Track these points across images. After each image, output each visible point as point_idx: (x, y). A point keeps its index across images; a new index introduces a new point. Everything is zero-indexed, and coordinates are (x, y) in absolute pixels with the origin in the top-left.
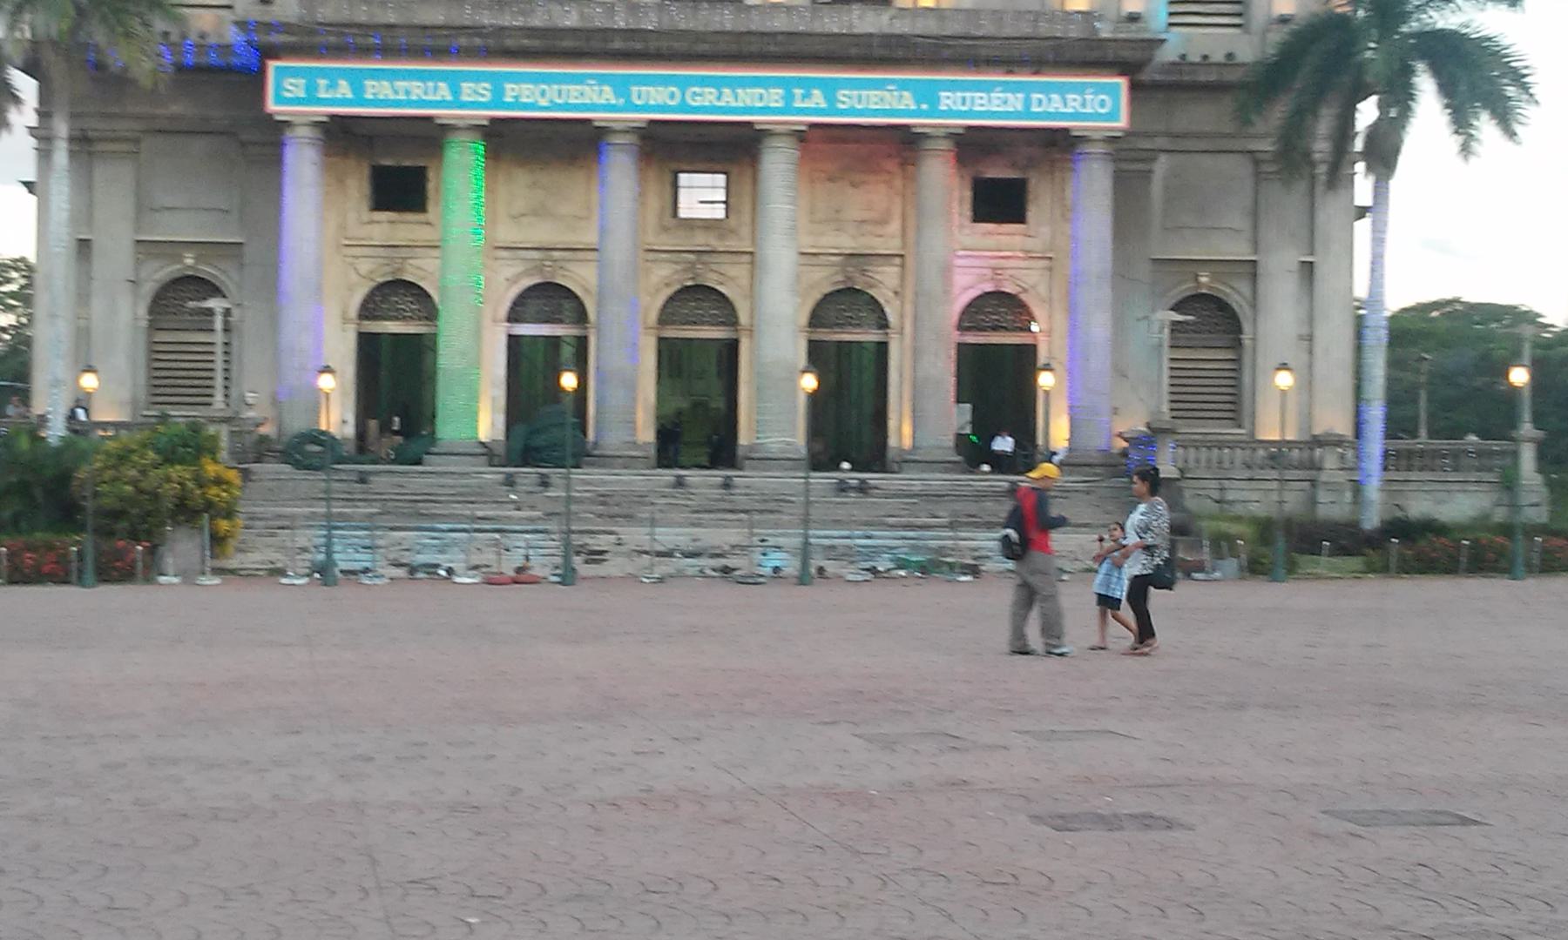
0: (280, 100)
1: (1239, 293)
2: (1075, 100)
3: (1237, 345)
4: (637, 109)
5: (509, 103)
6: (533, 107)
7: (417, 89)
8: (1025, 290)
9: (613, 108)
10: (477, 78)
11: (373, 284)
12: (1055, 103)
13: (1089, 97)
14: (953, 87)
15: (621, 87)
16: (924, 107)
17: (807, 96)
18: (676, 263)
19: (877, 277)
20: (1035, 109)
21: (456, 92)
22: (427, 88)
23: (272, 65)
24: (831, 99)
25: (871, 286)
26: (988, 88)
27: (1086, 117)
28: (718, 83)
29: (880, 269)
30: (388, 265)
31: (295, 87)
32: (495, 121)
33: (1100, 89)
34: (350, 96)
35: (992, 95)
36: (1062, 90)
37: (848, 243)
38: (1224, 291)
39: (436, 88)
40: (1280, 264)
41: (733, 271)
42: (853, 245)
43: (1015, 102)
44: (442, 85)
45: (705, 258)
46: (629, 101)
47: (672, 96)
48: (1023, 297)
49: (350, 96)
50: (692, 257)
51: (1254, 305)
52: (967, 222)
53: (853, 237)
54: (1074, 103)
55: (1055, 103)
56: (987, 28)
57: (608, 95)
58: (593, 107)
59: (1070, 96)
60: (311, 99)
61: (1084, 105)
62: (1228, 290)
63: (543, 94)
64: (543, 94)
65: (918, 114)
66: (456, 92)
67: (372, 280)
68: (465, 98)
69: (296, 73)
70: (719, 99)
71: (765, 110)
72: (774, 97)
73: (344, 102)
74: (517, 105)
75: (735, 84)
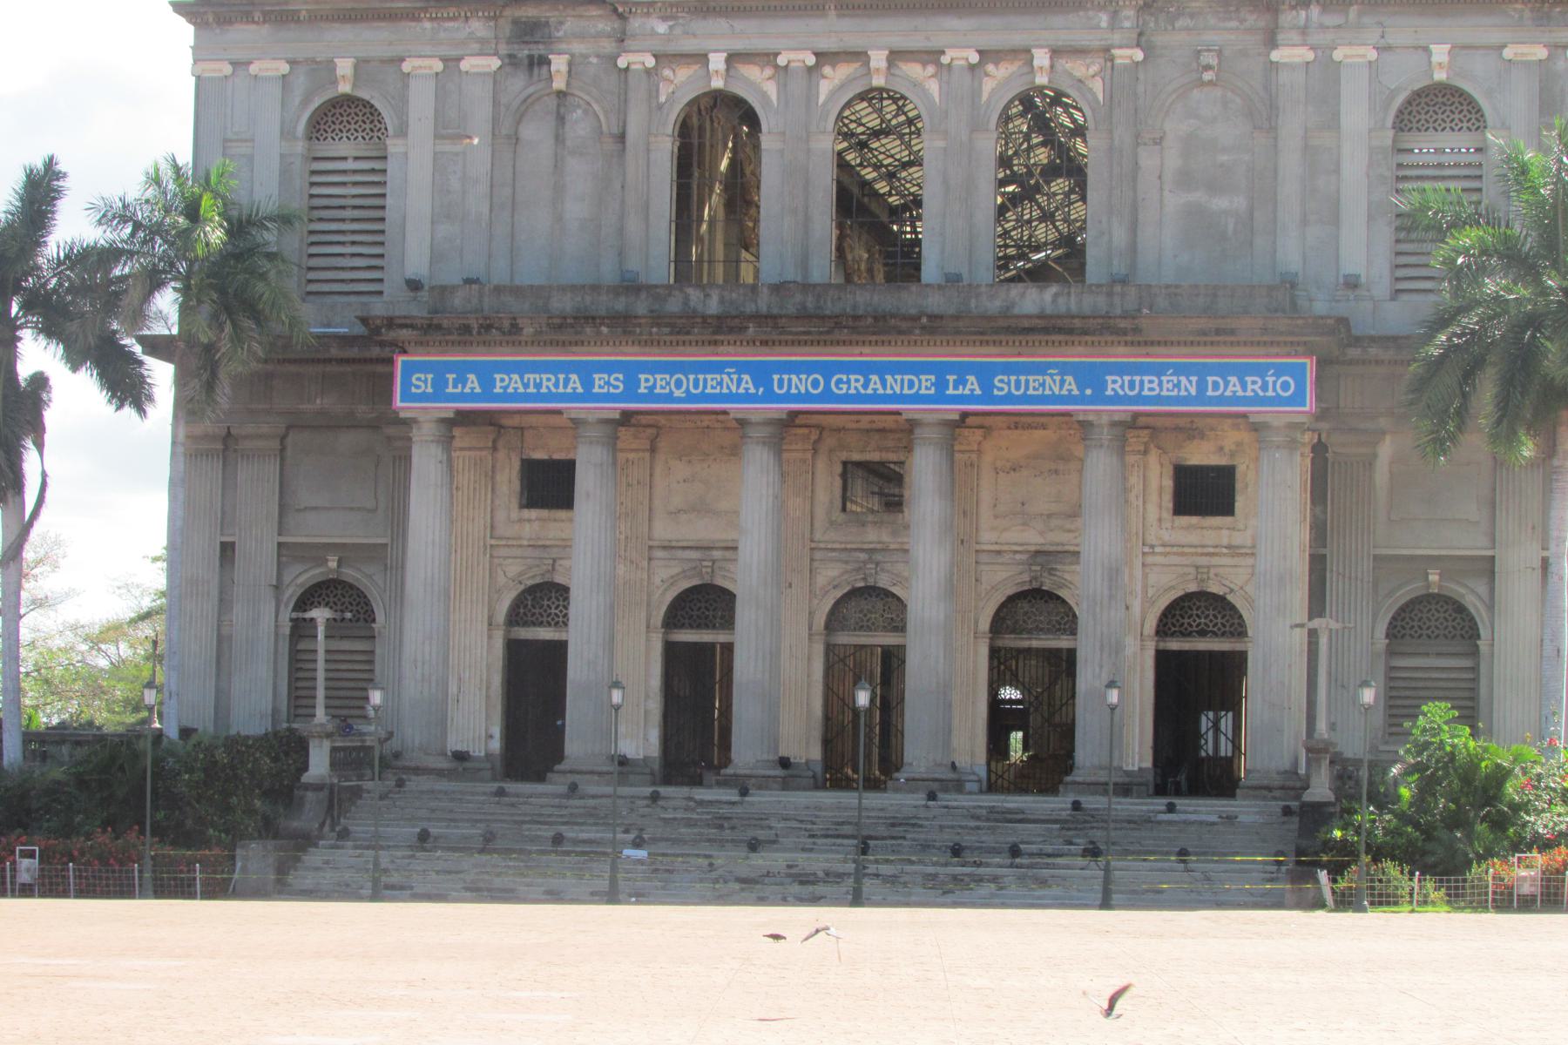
0: (407, 396)
1: (1473, 591)
2: (1254, 383)
3: (1474, 653)
5: (643, 394)
6: (669, 397)
7: (548, 382)
8: (1232, 590)
9: (748, 397)
10: (608, 368)
11: (522, 587)
13: (1270, 380)
15: (761, 375)
16: (1088, 392)
18: (846, 562)
19: (1067, 576)
20: (1210, 393)
21: (588, 383)
22: (557, 379)
23: (400, 360)
25: (1061, 586)
28: (865, 370)
29: (1067, 568)
30: (538, 566)
31: (422, 383)
33: (1280, 371)
35: (1164, 379)
36: (1242, 372)
37: (1033, 538)
38: (1456, 590)
39: (567, 381)
40: (1517, 559)
42: (1041, 541)
45: (878, 557)
46: (769, 390)
47: (815, 384)
48: (1229, 597)
50: (863, 556)
51: (1491, 607)
52: (1167, 515)
53: (1042, 533)
58: (730, 397)
59: (1249, 379)
60: (439, 394)
61: (1264, 387)
62: (1462, 590)
63: (679, 384)
64: (679, 384)
65: (1082, 399)
66: (588, 383)
67: (520, 583)
68: (596, 390)
69: (424, 367)
70: (865, 386)
71: (917, 398)
73: (472, 397)
74: (651, 396)
75: (882, 370)
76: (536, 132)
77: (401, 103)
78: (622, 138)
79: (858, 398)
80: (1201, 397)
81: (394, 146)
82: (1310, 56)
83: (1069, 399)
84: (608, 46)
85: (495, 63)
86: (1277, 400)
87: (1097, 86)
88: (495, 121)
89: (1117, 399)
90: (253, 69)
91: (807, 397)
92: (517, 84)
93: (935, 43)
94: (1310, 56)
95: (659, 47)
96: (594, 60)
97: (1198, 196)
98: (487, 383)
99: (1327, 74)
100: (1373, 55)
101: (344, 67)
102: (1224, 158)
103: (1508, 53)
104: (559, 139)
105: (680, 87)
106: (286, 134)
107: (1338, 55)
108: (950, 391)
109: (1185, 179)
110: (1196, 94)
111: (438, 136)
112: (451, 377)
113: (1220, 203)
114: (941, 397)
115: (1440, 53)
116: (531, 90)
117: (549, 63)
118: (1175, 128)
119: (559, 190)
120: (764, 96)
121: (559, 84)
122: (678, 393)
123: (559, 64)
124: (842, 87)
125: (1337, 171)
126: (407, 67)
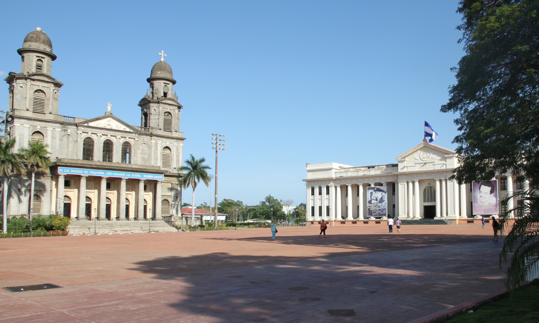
0: (59, 172)
4: (107, 175)
6: (94, 174)
9: (104, 175)
12: (157, 177)
14: (145, 175)
17: (128, 175)
20: (154, 178)
23: (59, 167)
24: (131, 175)
26: (149, 175)
27: (160, 179)
32: (89, 176)
34: (69, 172)
39: (81, 171)
41: (111, 195)
43: (152, 177)
44: (82, 171)
46: (106, 174)
47: (111, 174)
49: (69, 172)
54: (159, 177)
55: (157, 177)
56: (148, 168)
57: (103, 173)
58: (102, 175)
63: (95, 173)
64: (95, 173)
71: (123, 176)
72: (124, 175)
73: (68, 172)
74: (91, 174)
76: (65, 139)
77: (46, 133)
78: (77, 141)
79: (116, 176)
80: (153, 178)
81: (45, 139)
82: (155, 142)
83: (140, 177)
84: (76, 130)
85: (60, 130)
86: (161, 179)
87: (133, 142)
88: (60, 137)
89: (145, 178)
90: (24, 126)
91: (110, 175)
92: (63, 133)
93: (116, 135)
94: (155, 142)
95: (83, 131)
96: (73, 131)
97: (143, 156)
98: (70, 171)
99: (156, 144)
100: (161, 143)
101: (39, 127)
102: (146, 152)
103: (174, 144)
104: (68, 140)
105: (85, 136)
106: (29, 135)
107: (158, 142)
108: (65, 171)
109: (142, 154)
110: (143, 144)
111: (52, 138)
112: (65, 170)
113: (145, 156)
114: (126, 176)
115: (168, 143)
116: (65, 134)
117: (68, 131)
118: (141, 148)
119: (68, 147)
120: (95, 138)
121: (69, 134)
122: (95, 174)
123: (69, 131)
124: (123, 140)
125: (157, 154)
126: (47, 128)
